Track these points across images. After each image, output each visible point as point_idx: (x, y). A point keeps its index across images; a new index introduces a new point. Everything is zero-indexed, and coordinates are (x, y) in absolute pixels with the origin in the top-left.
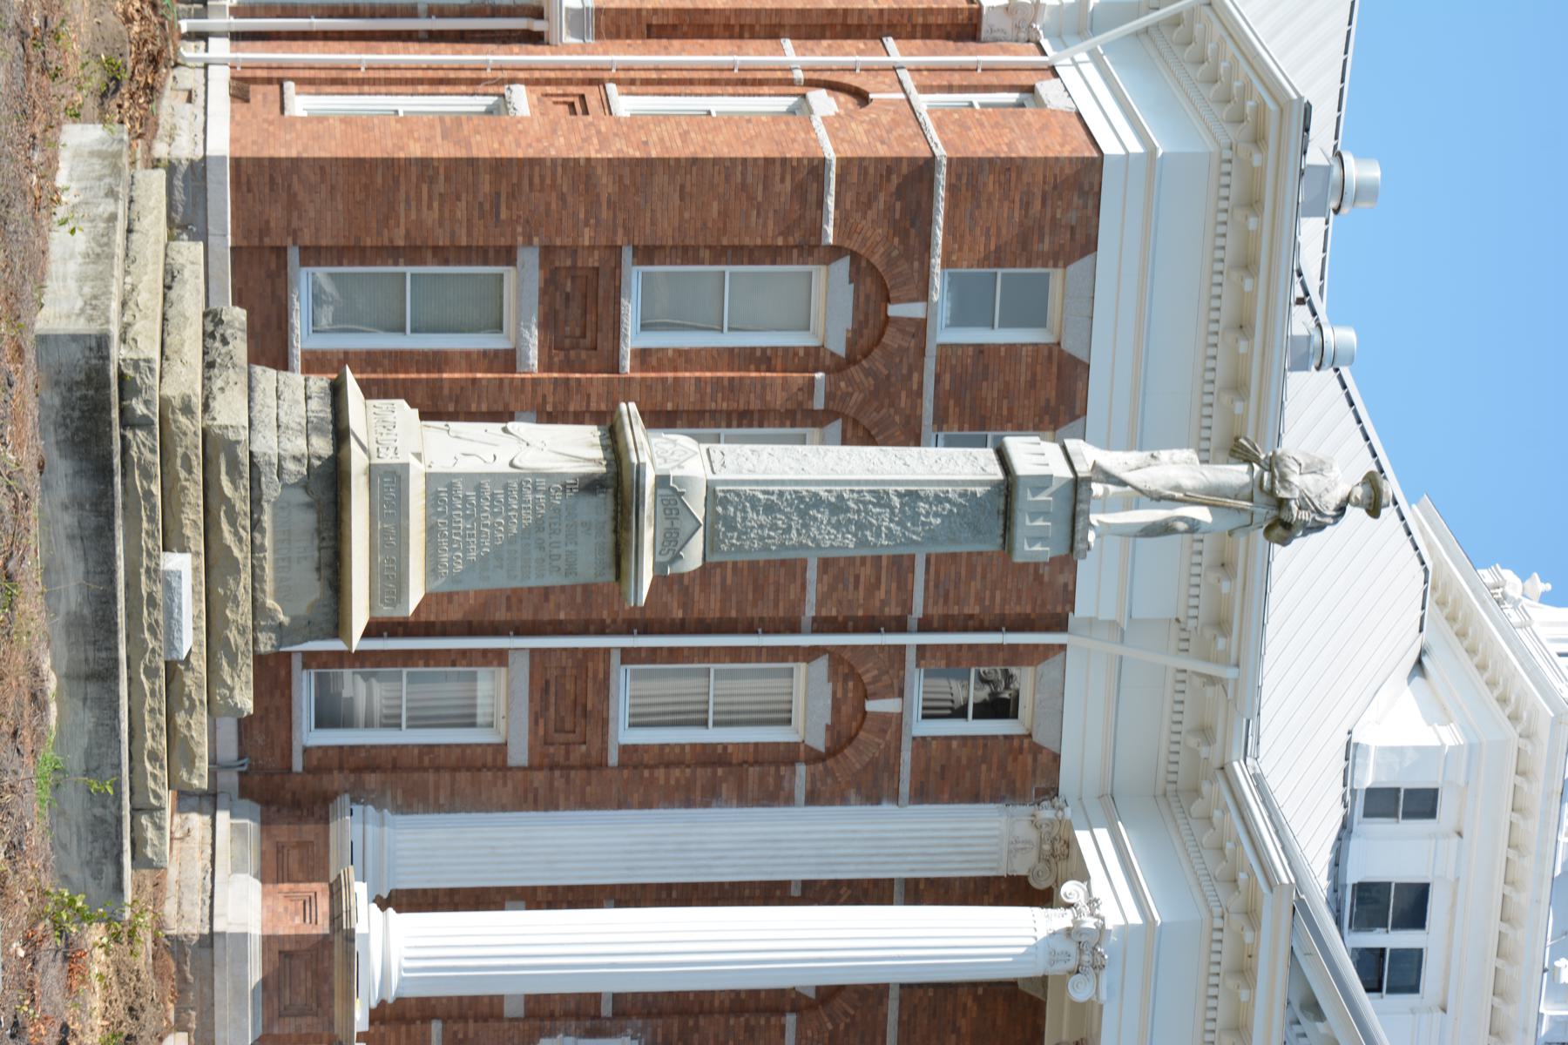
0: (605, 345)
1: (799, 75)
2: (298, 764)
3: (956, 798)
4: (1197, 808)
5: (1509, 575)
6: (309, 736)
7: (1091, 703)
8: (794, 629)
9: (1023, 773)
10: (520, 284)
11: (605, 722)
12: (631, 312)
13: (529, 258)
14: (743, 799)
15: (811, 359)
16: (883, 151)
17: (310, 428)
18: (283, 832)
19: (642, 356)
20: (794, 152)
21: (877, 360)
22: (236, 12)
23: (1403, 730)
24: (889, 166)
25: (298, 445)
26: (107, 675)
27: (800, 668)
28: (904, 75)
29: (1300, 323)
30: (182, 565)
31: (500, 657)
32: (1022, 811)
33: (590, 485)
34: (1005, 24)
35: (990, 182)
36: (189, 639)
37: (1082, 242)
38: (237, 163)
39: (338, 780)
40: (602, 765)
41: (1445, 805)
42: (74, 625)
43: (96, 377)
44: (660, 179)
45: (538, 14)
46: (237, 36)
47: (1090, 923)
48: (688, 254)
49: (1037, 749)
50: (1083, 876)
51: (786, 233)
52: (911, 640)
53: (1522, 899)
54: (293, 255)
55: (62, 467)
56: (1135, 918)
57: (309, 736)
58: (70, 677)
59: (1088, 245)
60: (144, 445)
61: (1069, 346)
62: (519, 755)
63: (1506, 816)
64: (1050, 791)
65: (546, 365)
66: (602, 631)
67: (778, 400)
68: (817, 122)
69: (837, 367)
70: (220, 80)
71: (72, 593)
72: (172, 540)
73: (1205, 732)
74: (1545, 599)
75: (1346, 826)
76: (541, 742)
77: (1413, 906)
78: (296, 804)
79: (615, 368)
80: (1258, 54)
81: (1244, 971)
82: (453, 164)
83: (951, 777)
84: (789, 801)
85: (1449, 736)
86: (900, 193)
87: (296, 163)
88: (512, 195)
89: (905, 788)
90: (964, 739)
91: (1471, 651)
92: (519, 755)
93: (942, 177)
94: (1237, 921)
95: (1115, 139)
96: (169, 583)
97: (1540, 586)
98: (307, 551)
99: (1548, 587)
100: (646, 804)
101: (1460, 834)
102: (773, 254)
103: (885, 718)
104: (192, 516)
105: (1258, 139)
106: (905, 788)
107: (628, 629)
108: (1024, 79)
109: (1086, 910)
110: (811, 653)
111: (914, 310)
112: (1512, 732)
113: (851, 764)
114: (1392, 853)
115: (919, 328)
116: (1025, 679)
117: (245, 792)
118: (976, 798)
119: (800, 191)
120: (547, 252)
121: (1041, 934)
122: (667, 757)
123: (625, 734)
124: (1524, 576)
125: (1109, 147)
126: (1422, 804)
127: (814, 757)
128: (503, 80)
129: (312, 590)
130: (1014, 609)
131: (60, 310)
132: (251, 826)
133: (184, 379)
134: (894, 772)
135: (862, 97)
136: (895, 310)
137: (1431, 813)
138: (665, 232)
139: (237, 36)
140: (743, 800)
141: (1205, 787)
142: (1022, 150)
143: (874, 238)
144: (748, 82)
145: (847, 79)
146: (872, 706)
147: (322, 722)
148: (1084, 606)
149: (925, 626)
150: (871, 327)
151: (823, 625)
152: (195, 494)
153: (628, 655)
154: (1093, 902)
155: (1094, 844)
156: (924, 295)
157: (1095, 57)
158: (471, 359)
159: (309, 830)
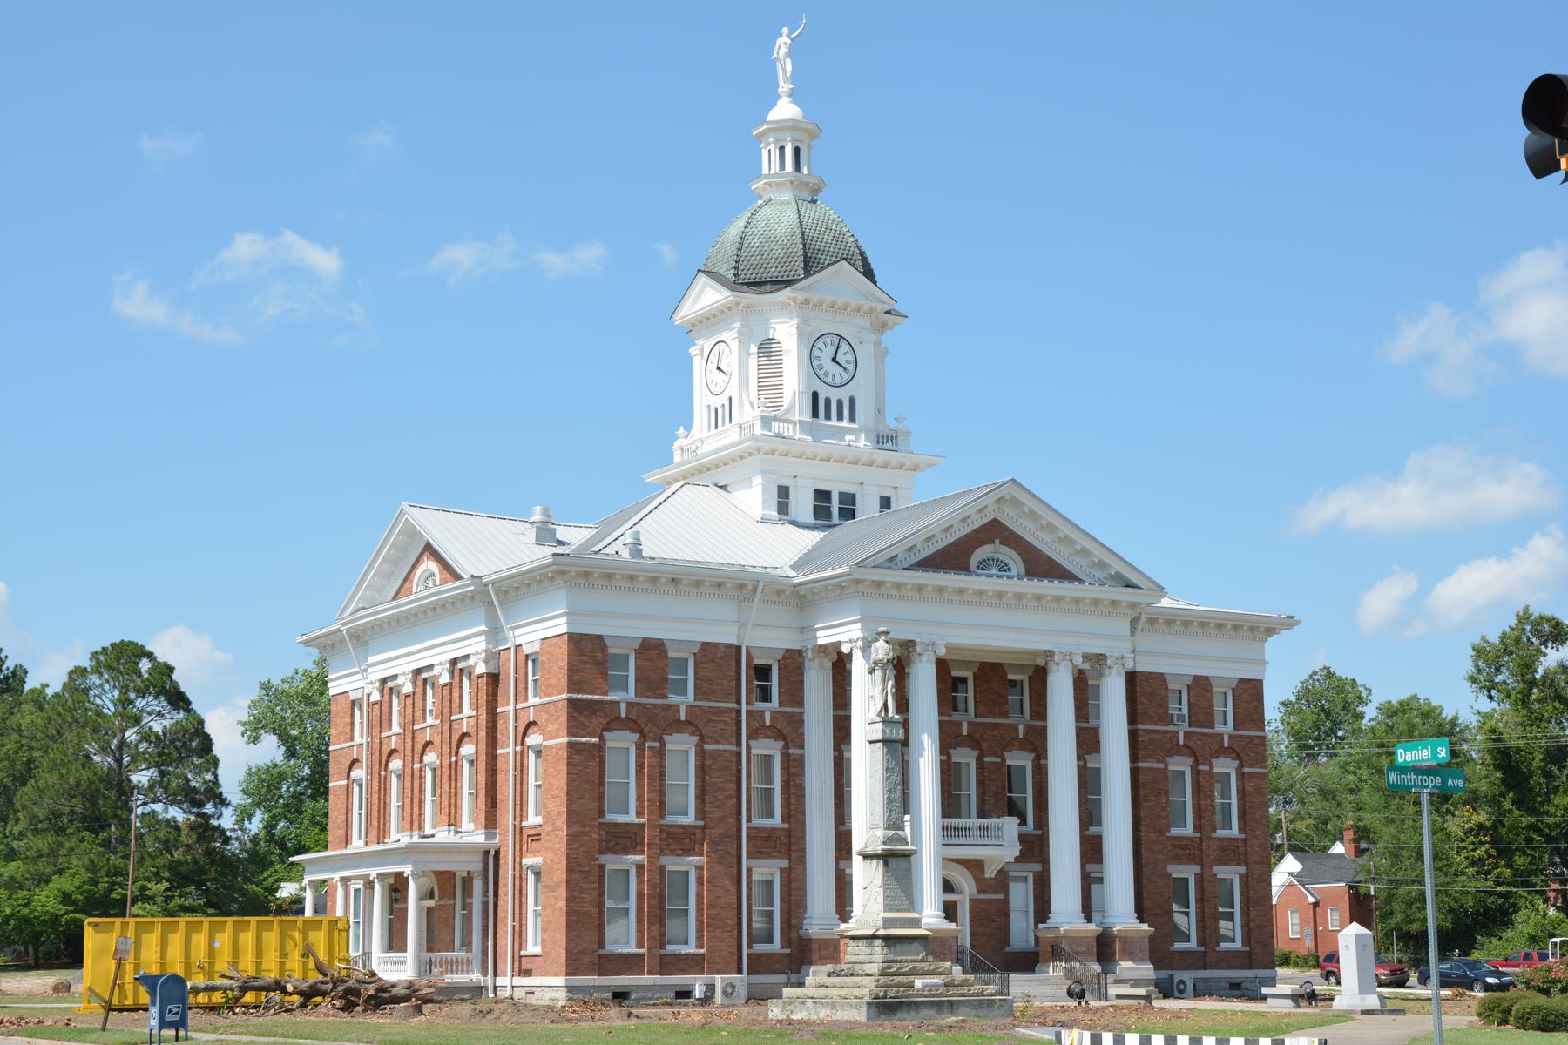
0: (635, 829)
2: (788, 951)
3: (802, 690)
4: (809, 596)
5: (677, 444)
6: (776, 946)
7: (766, 637)
8: (739, 754)
9: (793, 663)
10: (612, 863)
11: (773, 830)
12: (622, 819)
13: (603, 859)
14: (802, 774)
15: (640, 747)
16: (564, 718)
17: (871, 945)
18: (815, 957)
19: (639, 814)
21: (642, 721)
22: (486, 975)
23: (753, 498)
24: (570, 717)
25: (878, 949)
26: (951, 1002)
27: (754, 751)
28: (519, 706)
29: (625, 554)
30: (919, 983)
31: (749, 870)
32: (807, 664)
33: (886, 864)
34: (492, 662)
35: (577, 677)
36: (937, 980)
37: (599, 640)
38: (568, 974)
39: (794, 935)
40: (789, 830)
41: (784, 483)
42: (939, 1012)
43: (878, 1005)
44: (574, 807)
45: (487, 852)
46: (495, 974)
47: (860, 643)
48: (602, 796)
49: (784, 658)
50: (839, 644)
51: (594, 757)
52: (744, 708)
53: (822, 454)
54: (601, 952)
55: (900, 1015)
56: (858, 625)
57: (776, 946)
58: (952, 1013)
59: (600, 637)
60: (891, 992)
61: (637, 646)
62: (785, 863)
63: (789, 459)
64: (800, 652)
65: (642, 852)
66: (740, 830)
67: (655, 761)
68: (546, 743)
69: (644, 737)
70: (518, 981)
71: (931, 1012)
72: (911, 985)
73: (779, 592)
74: (689, 428)
75: (793, 523)
76: (779, 854)
77: (822, 496)
78: (803, 951)
79: (643, 825)
81: (879, 584)
82: (569, 889)
83: (794, 693)
84: (803, 756)
85: (758, 481)
86: (580, 712)
87: (568, 951)
88: (580, 865)
89: (797, 710)
90: (780, 686)
91: (717, 466)
92: (785, 863)
93: (575, 696)
94: (860, 587)
95: (560, 627)
96: (925, 986)
97: (682, 431)
98: (906, 947)
100: (804, 813)
102: (602, 763)
103: (772, 718)
104: (905, 979)
105: (563, 573)
106: (797, 710)
107: (739, 820)
108: (521, 658)
110: (749, 748)
111: (623, 707)
113: (790, 732)
114: (803, 504)
115: (629, 704)
116: (757, 661)
117: (798, 972)
118: (802, 682)
119: (579, 752)
120: (601, 852)
122: (786, 804)
123: (777, 821)
125: (564, 629)
126: (784, 492)
127: (786, 746)
128: (518, 865)
129: (916, 946)
130: (733, 668)
131: (861, 1015)
132: (812, 968)
133: (870, 982)
134: (792, 714)
135: (530, 725)
136: (623, 715)
137: (787, 488)
138: (593, 805)
139: (495, 974)
140: (802, 774)
142: (564, 664)
143: (597, 722)
144: (521, 769)
145: (521, 729)
146: (768, 723)
147: (770, 941)
148: (734, 641)
149: (739, 702)
150: (630, 724)
151: (739, 744)
152: (899, 978)
153: (749, 820)
155: (824, 638)
156: (617, 703)
158: (640, 883)
159: (815, 946)
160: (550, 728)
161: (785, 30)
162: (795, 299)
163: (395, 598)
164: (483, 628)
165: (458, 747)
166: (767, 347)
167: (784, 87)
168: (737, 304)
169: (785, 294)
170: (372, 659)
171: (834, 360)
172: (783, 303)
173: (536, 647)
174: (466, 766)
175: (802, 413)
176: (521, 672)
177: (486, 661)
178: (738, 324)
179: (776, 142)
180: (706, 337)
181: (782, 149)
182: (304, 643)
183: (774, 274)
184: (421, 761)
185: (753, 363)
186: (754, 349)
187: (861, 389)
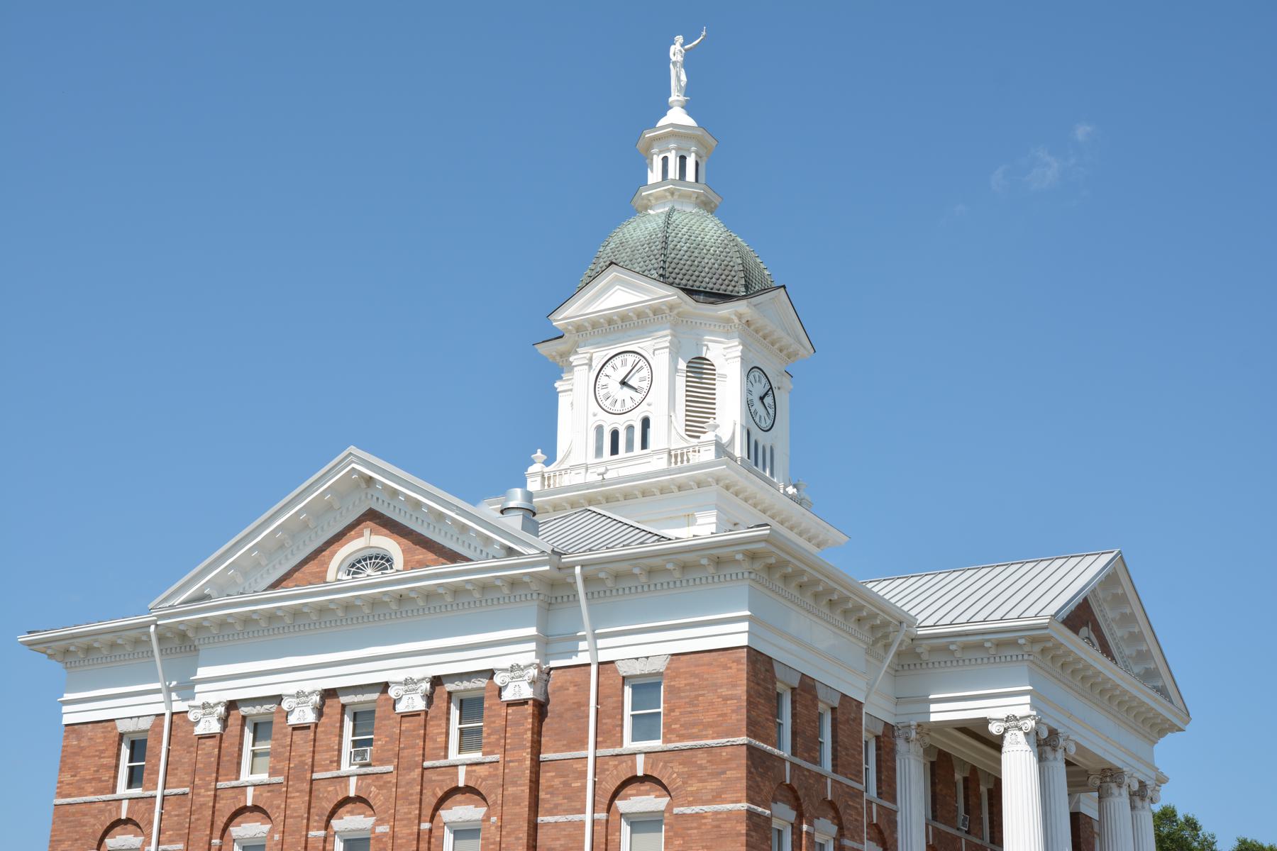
1: (602, 816)
4: (925, 657)
5: (531, 469)
9: (886, 741)
20: (742, 828)
21: (801, 793)
34: (540, 684)
50: (985, 722)
69: (800, 816)
86: (756, 768)
95: (737, 636)
105: (753, 556)
109: (1013, 723)
112: (715, 487)
121: (1029, 748)
124: (532, 462)
125: (743, 640)
141: (918, 650)
142: (741, 691)
154: (1008, 719)
155: (941, 713)
157: (597, 637)
160: (694, 786)
162: (740, 316)
163: (274, 586)
164: (532, 631)
165: (437, 807)
166: (699, 367)
167: (676, 96)
168: (671, 308)
169: (725, 310)
170: (202, 672)
171: (762, 399)
172: (728, 321)
173: (660, 666)
174: (448, 838)
175: (739, 450)
176: (610, 703)
177: (533, 683)
178: (668, 332)
179: (677, 149)
180: (598, 344)
181: (683, 159)
182: (30, 644)
183: (708, 284)
184: (327, 826)
185: (681, 381)
186: (682, 365)
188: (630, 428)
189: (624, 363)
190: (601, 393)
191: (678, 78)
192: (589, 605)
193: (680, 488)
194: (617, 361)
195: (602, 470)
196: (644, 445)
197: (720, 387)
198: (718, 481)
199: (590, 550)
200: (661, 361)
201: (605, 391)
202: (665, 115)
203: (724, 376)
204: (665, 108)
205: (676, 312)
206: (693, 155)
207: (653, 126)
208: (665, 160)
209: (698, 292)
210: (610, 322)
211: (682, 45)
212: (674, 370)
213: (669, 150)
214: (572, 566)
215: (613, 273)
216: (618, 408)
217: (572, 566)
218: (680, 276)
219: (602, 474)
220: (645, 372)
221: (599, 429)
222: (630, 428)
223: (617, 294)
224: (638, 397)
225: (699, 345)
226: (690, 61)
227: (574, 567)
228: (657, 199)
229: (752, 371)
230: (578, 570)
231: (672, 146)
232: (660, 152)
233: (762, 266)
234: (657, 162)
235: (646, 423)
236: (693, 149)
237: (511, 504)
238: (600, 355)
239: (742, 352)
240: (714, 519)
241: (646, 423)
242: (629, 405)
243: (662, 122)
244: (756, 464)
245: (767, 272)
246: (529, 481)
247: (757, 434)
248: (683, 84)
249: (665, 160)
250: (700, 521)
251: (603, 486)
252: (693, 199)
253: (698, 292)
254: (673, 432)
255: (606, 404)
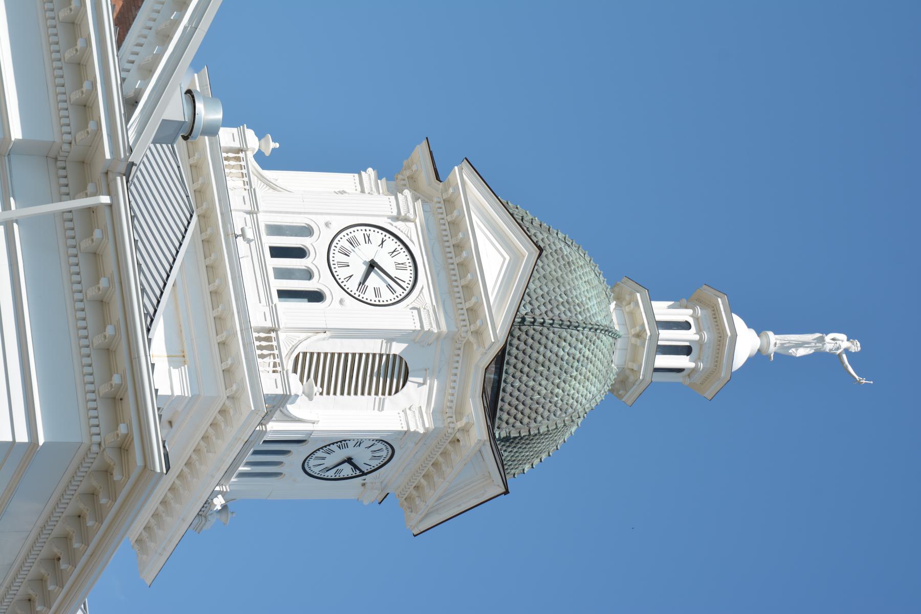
5: (250, 134)
80: (139, 357)
99: (277, 145)
101: (170, 423)
105: (123, 448)
112: (224, 394)
124: (260, 136)
161: (856, 347)
162: (465, 430)
166: (393, 373)
167: (774, 340)
168: (477, 333)
169: (475, 410)
171: (349, 460)
172: (459, 413)
175: (276, 427)
178: (444, 328)
179: (700, 343)
180: (427, 230)
181: (686, 350)
185: (374, 346)
186: (397, 348)
187: (291, 486)
188: (308, 274)
189: (399, 266)
190: (359, 234)
191: (801, 345)
192: (54, 214)
193: (223, 344)
194: (403, 257)
195: (250, 234)
196: (284, 294)
197: (366, 401)
198: (231, 398)
199: (143, 290)
200: (402, 318)
201: (361, 239)
202: (749, 327)
203: (381, 408)
204: (758, 325)
205: (472, 339)
206: (692, 365)
207: (734, 308)
208: (686, 326)
209: (499, 371)
210: (459, 247)
211: (846, 351)
212: (390, 337)
213: (699, 331)
214: (110, 191)
215: (527, 252)
216: (337, 257)
217: (110, 191)
218: (522, 346)
219: (243, 235)
220: (387, 296)
221: (307, 231)
222: (308, 274)
223: (496, 258)
224: (352, 285)
225: (426, 372)
226: (824, 361)
227: (109, 194)
228: (632, 314)
229: (387, 447)
230: (105, 199)
231: (706, 336)
232: (697, 319)
233: (536, 462)
234: (683, 315)
235: (316, 297)
236: (701, 365)
237: (200, 106)
238: (411, 232)
239: (416, 433)
240: (177, 392)
241: (316, 297)
242: (342, 273)
243: (739, 322)
244: (256, 453)
245: (527, 467)
246: (235, 130)
247: (299, 453)
248: (792, 351)
249: (686, 326)
250: (175, 372)
251: (227, 235)
252: (630, 365)
253: (499, 371)
254: (303, 335)
255: (343, 242)
